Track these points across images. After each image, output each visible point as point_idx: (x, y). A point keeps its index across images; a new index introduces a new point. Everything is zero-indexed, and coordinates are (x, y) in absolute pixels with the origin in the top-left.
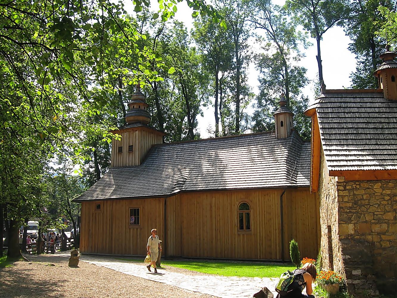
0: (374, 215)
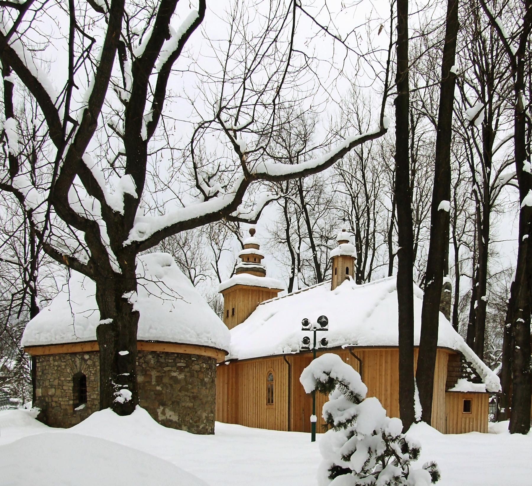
0: (50, 381)
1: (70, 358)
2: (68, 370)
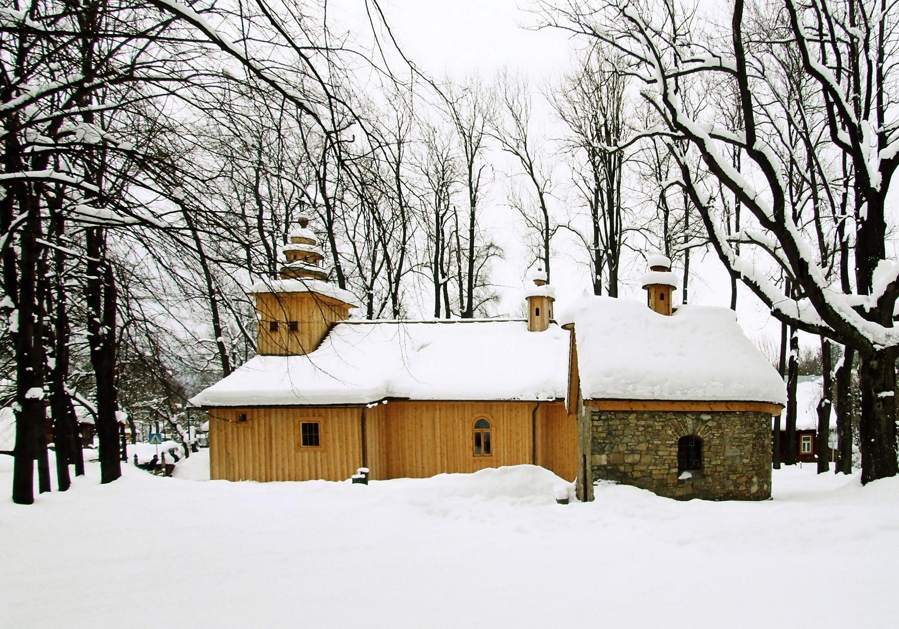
2: (670, 432)
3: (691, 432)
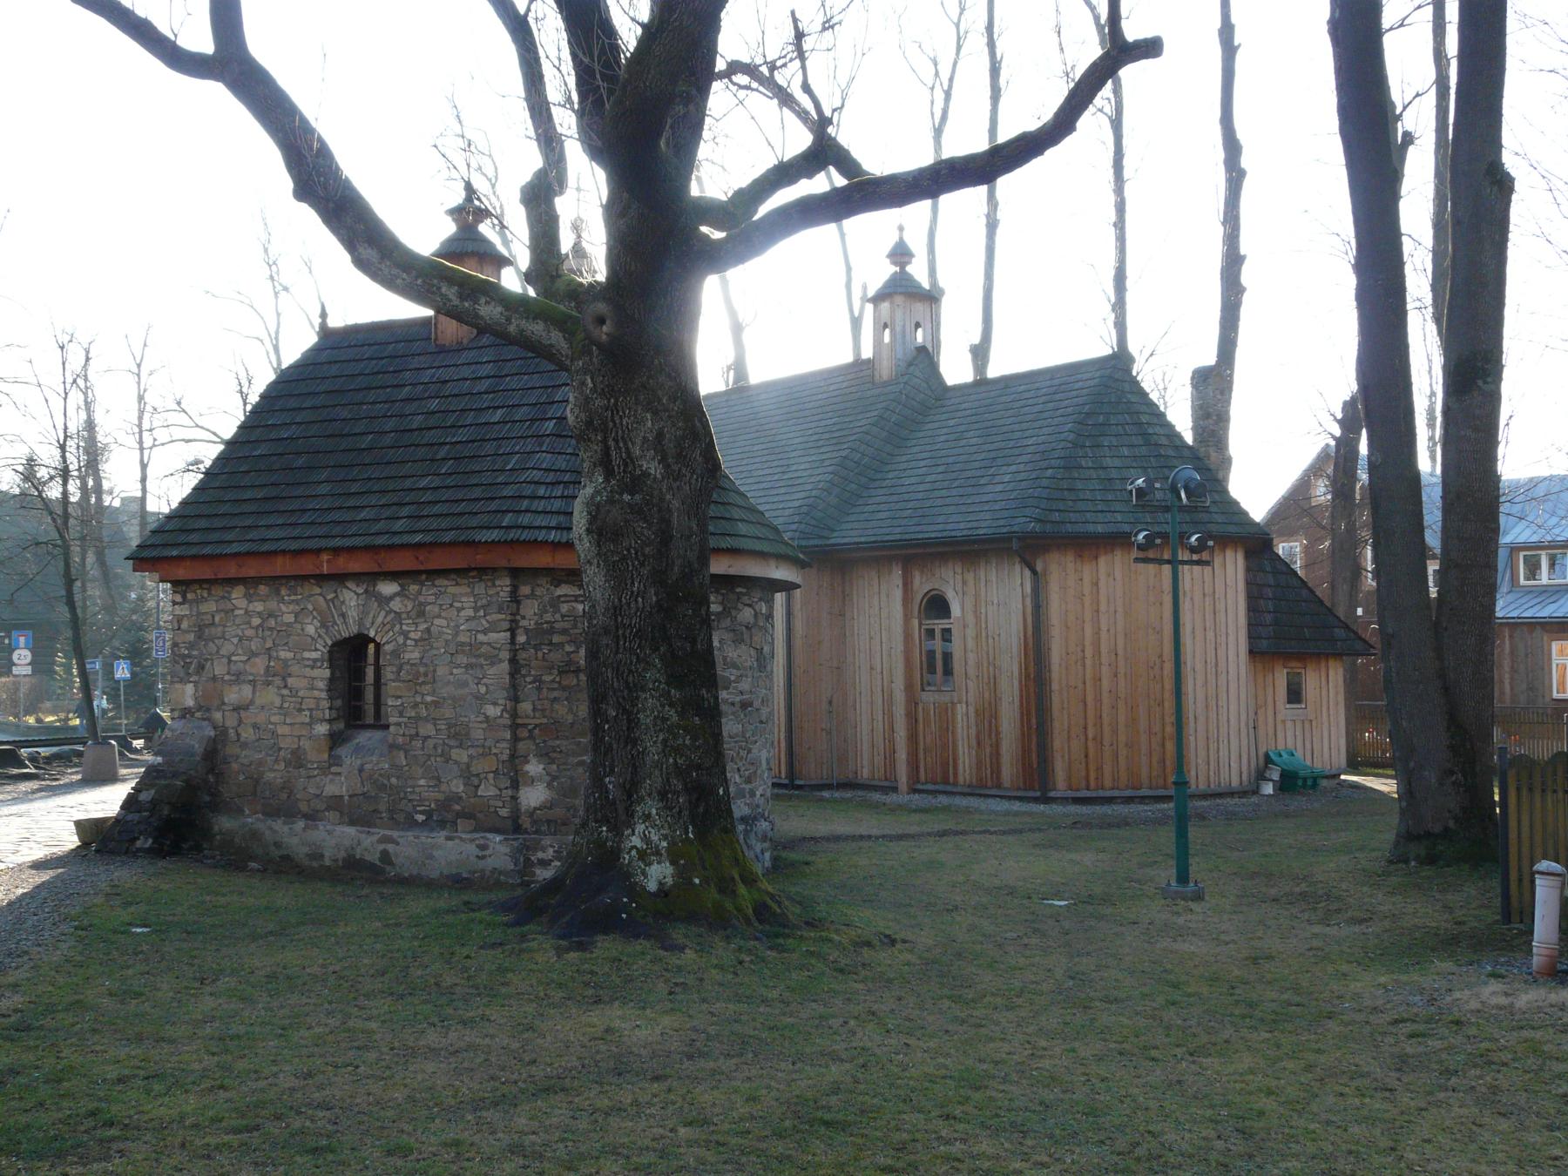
0: (230, 661)
1: (318, 590)
2: (311, 630)
3: (354, 630)
